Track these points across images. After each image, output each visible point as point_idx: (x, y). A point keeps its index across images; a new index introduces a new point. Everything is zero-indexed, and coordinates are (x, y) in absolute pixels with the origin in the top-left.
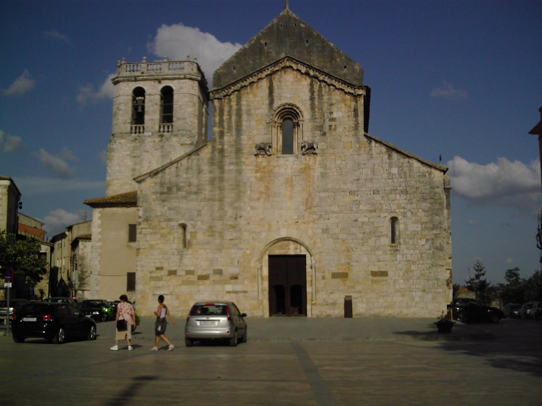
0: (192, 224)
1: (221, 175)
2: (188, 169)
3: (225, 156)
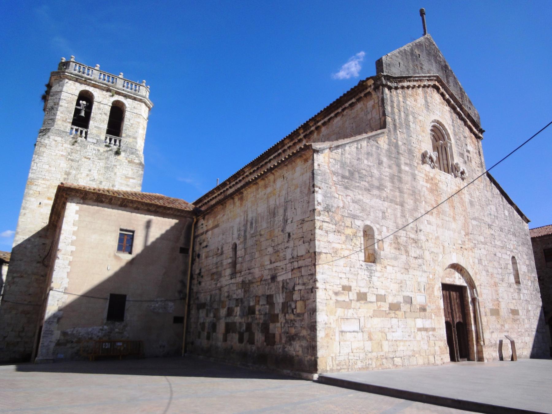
0: (378, 229)
1: (399, 175)
2: (368, 154)
3: (400, 153)
